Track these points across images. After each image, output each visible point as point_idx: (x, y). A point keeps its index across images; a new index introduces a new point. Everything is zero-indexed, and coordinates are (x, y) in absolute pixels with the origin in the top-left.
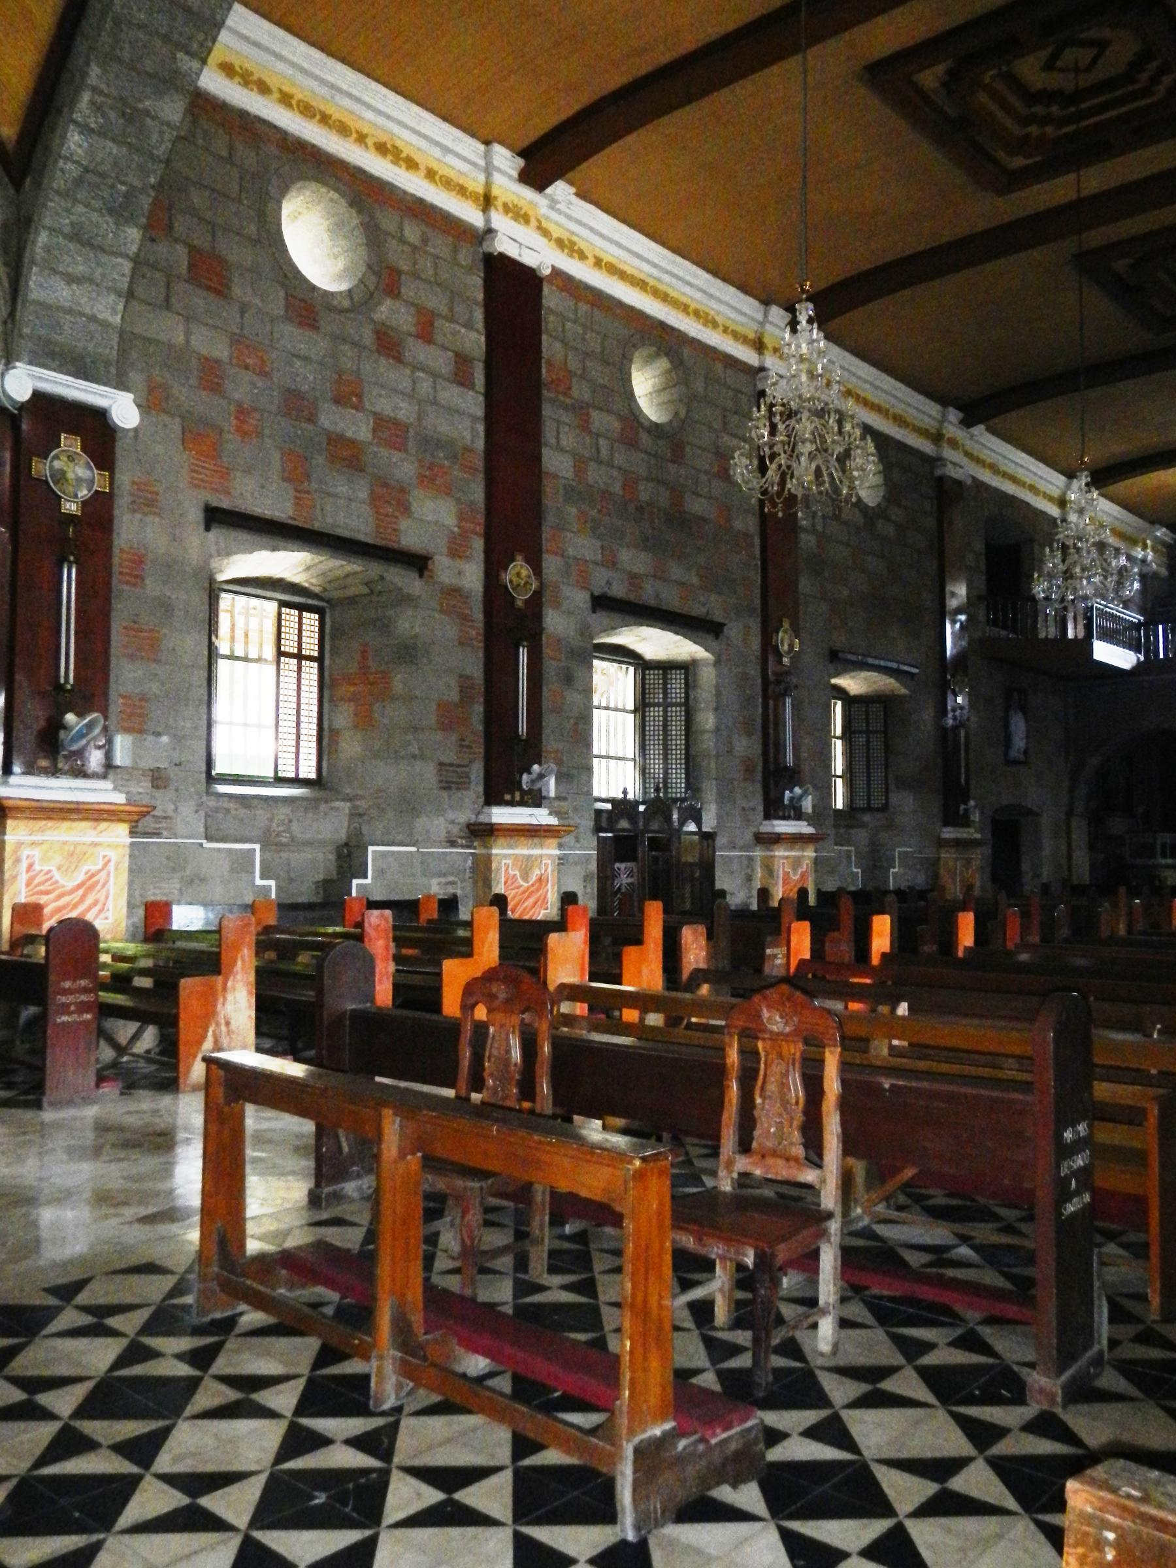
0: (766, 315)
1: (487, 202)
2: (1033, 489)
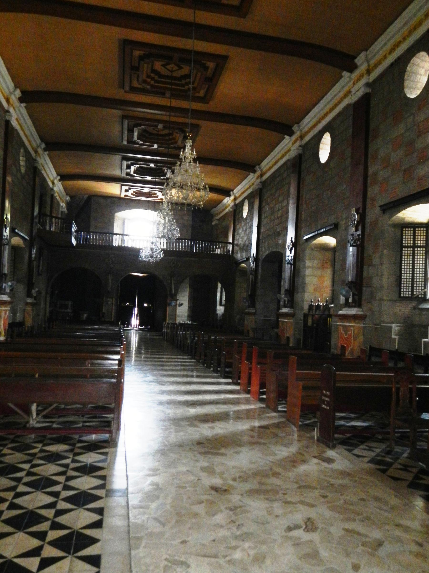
0: (14, 91)
2: (48, 175)
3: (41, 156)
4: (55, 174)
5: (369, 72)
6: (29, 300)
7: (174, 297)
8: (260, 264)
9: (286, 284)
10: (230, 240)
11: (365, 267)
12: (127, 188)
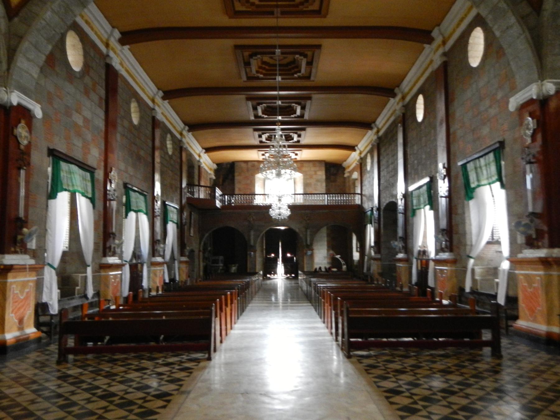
0: (157, 93)
1: (107, 45)
2: (194, 150)
3: (186, 136)
4: (200, 149)
5: (444, 43)
6: (184, 259)
7: (310, 247)
8: (382, 213)
9: (400, 233)
10: (359, 192)
11: (453, 216)
12: (263, 152)
